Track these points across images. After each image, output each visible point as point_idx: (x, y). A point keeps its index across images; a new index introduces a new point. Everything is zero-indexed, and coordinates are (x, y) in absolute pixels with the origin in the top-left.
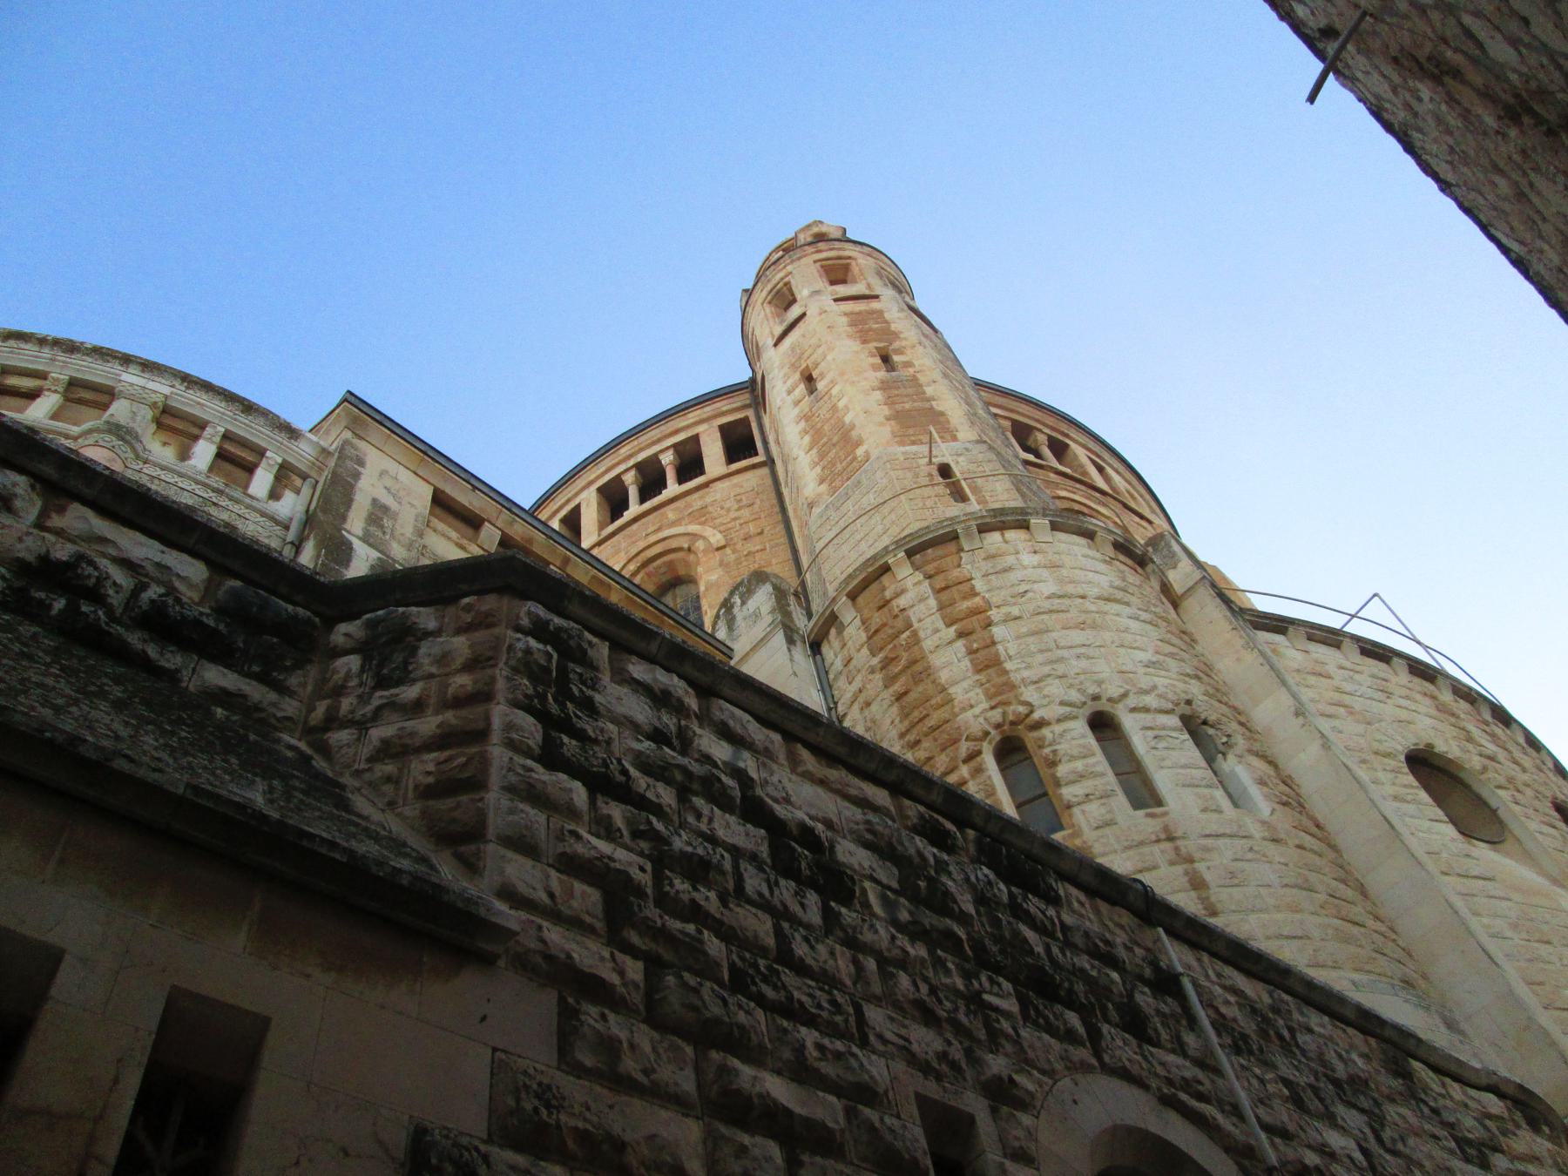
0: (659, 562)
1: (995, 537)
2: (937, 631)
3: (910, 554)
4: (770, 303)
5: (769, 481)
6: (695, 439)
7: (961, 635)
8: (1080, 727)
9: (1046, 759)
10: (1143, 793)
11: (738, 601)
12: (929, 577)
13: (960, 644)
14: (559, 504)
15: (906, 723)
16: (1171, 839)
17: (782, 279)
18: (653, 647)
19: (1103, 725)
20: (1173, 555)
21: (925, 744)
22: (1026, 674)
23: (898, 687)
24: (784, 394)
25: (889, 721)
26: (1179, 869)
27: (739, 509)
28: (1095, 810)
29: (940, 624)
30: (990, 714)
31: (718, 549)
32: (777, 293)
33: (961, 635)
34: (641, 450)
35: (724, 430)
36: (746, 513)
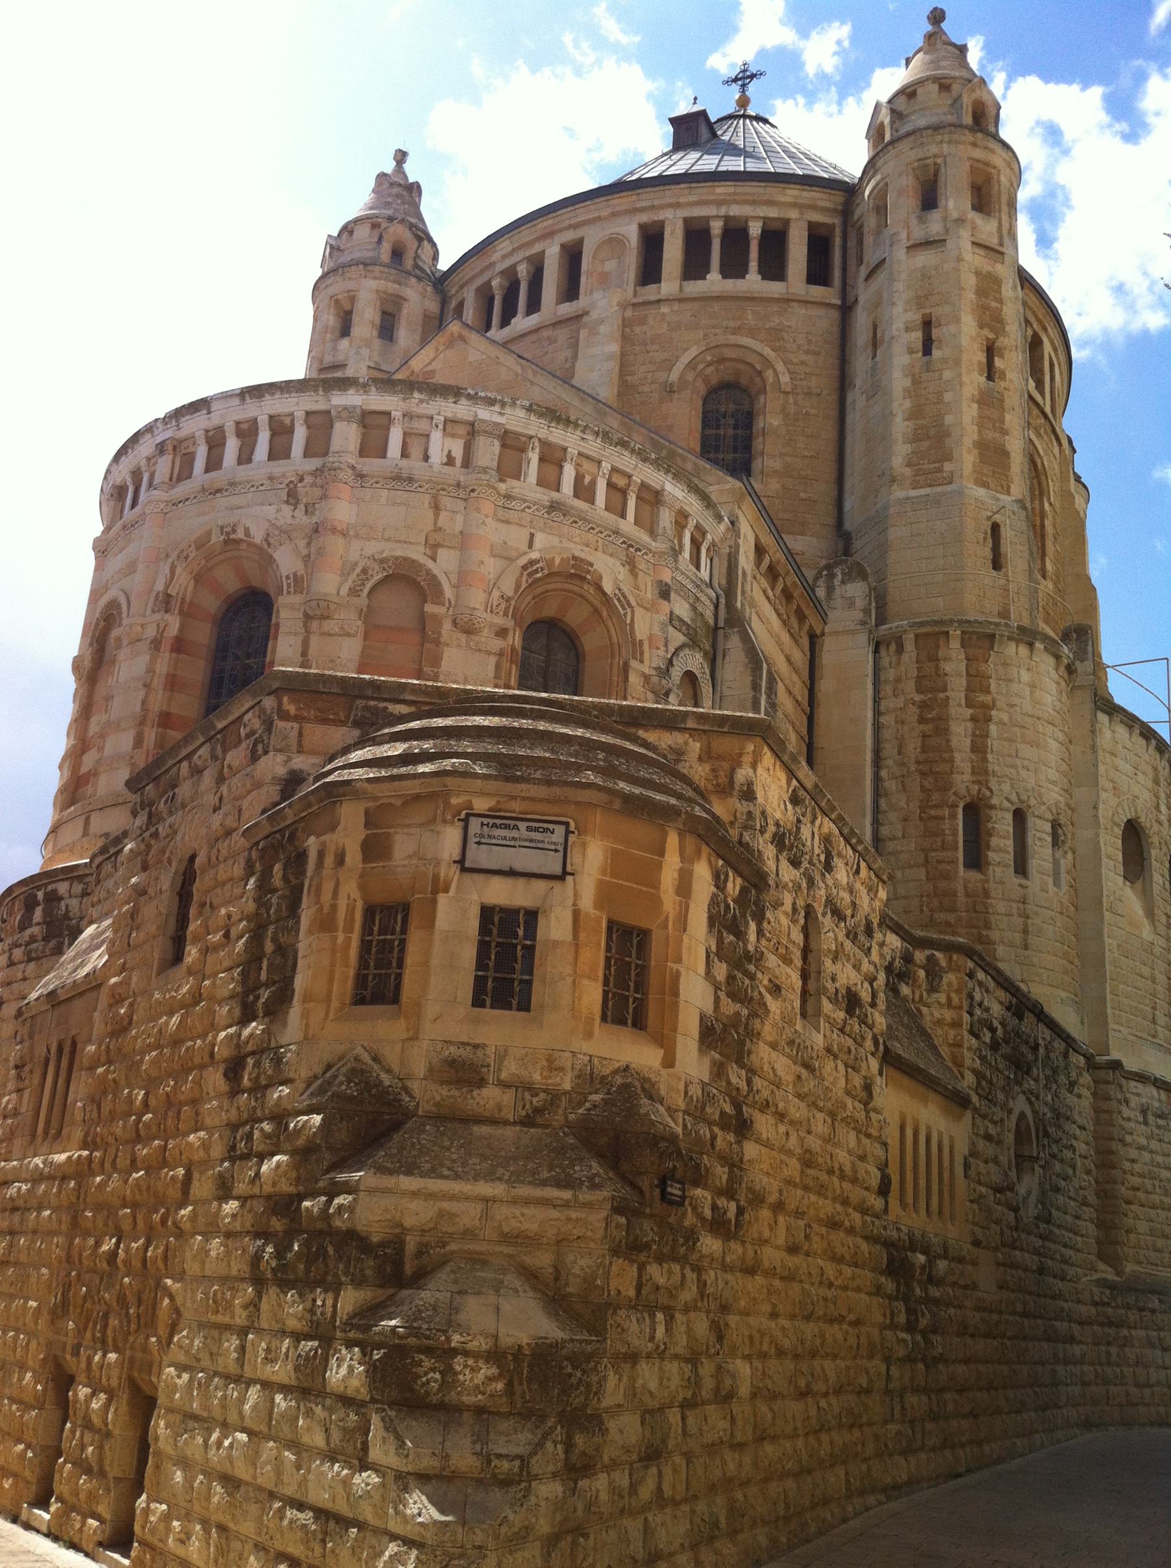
0: (727, 364)
1: (1011, 648)
2: (960, 705)
3: (963, 633)
4: (913, 169)
5: (836, 330)
6: (786, 222)
7: (973, 719)
8: (1009, 817)
9: (988, 830)
10: (1021, 867)
11: (840, 576)
12: (968, 659)
13: (970, 725)
14: (644, 204)
15: (924, 756)
16: (1024, 903)
17: (935, 156)
18: (983, 964)
19: (1020, 816)
20: (1086, 652)
21: (930, 779)
22: (996, 768)
23: (928, 728)
24: (901, 326)
25: (913, 746)
26: (1021, 920)
27: (807, 352)
28: (998, 870)
29: (963, 702)
30: (971, 786)
31: (785, 393)
32: (926, 166)
33: (973, 719)
34: (736, 202)
35: (812, 226)
36: (809, 359)
